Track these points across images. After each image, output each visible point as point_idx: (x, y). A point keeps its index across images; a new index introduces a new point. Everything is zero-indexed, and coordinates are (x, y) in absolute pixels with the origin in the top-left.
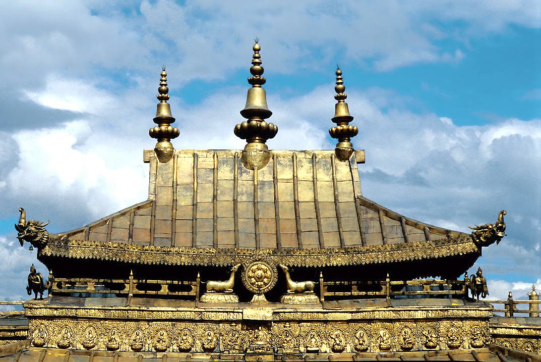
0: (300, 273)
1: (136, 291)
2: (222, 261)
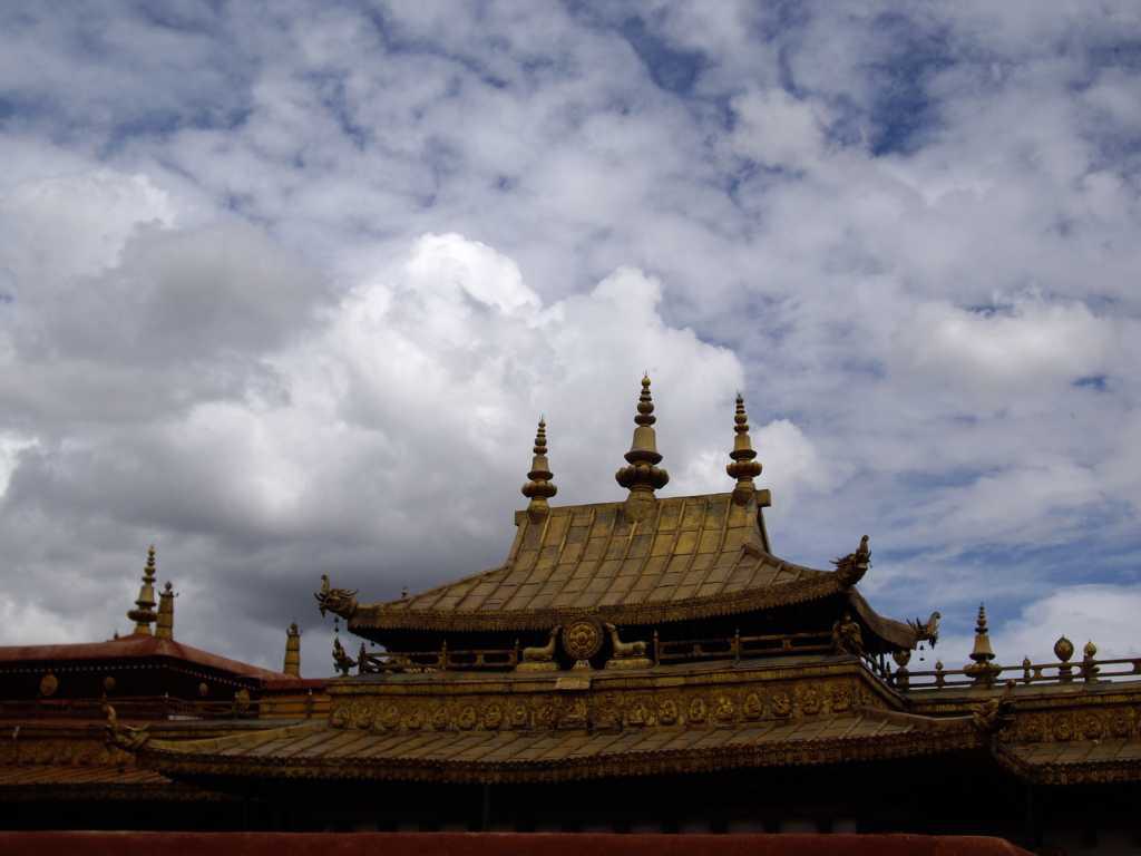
0: (628, 633)
1: (450, 663)
2: (541, 624)
